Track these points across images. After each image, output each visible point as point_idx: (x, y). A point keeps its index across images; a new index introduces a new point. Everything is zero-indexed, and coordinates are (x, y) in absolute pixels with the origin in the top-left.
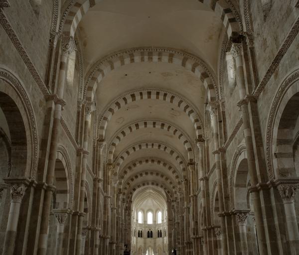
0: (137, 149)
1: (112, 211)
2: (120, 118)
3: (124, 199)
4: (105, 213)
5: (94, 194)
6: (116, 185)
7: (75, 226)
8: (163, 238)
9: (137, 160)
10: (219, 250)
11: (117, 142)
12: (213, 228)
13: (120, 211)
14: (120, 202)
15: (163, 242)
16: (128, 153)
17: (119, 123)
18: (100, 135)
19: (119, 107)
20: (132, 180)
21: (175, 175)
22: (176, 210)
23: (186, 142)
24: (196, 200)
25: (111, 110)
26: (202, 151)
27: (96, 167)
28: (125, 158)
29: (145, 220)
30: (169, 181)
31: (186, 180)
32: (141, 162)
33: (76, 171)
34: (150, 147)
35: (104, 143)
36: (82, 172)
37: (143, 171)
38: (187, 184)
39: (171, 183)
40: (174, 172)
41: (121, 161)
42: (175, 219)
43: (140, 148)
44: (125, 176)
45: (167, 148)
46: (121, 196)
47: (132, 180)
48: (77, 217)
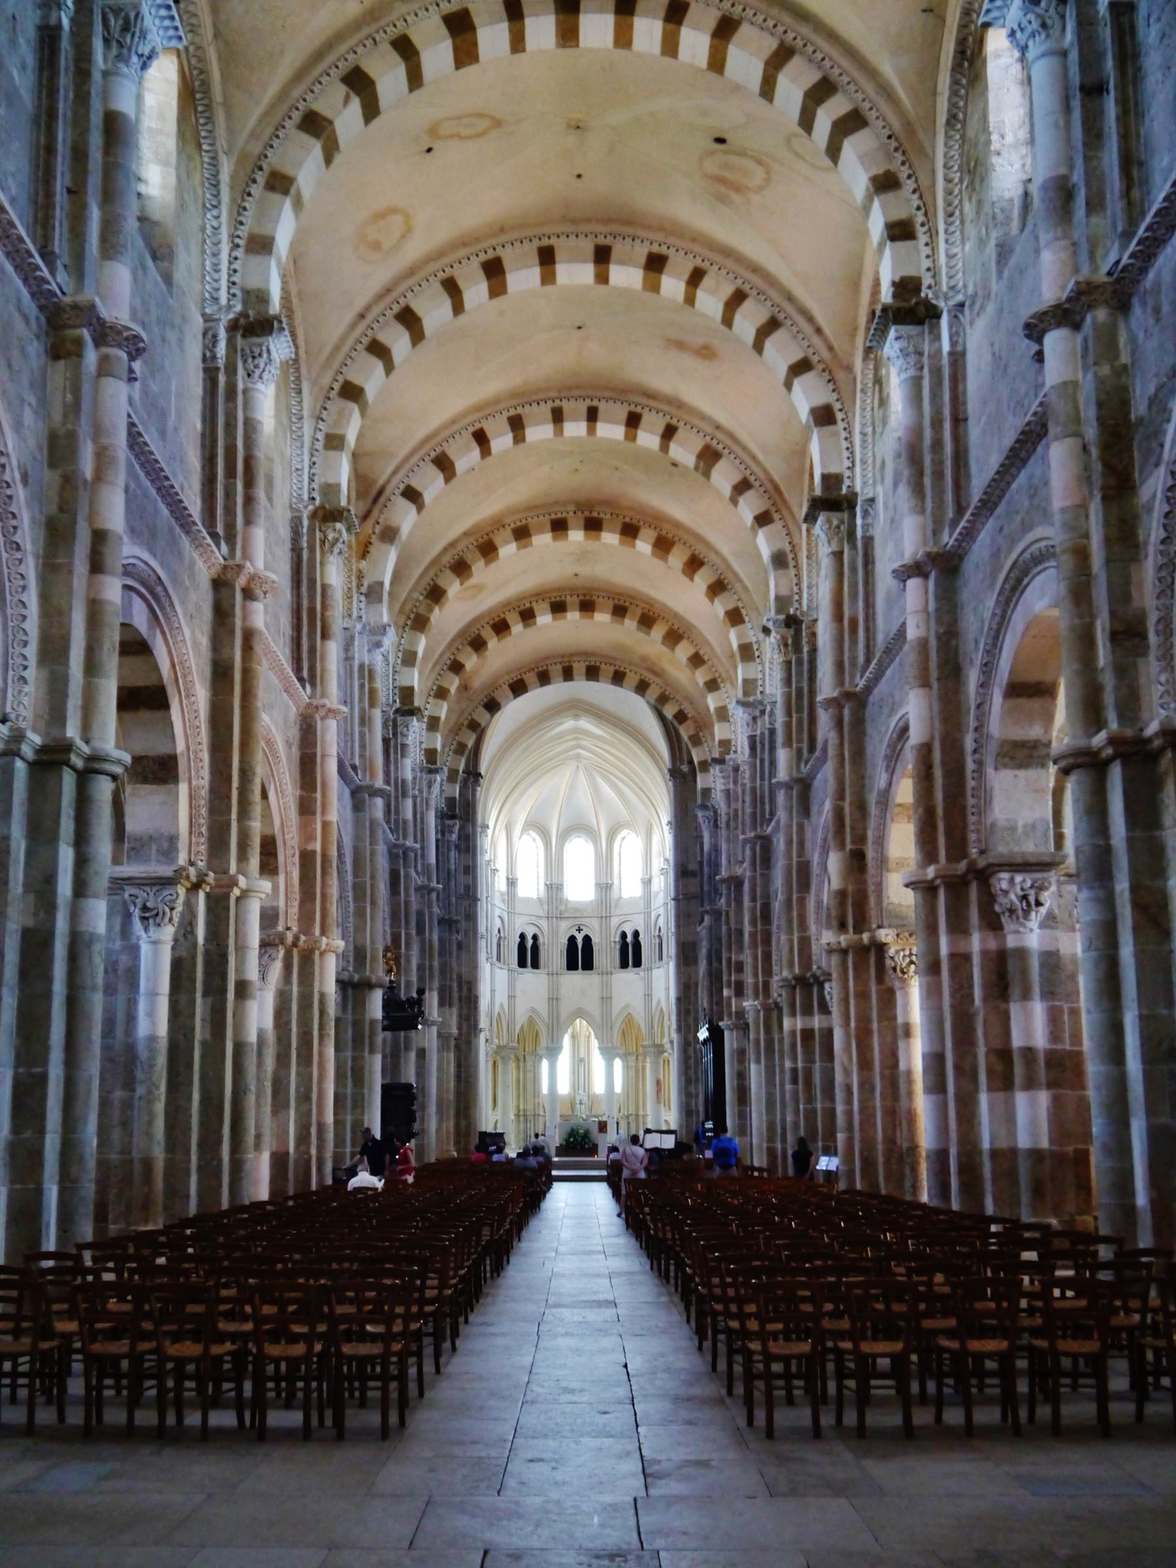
0: (501, 442)
1: (358, 806)
2: (380, 216)
3: (431, 755)
4: (306, 808)
5: (220, 674)
6: (378, 659)
7: (54, 839)
8: (650, 969)
9: (498, 523)
10: (1015, 1009)
11: (372, 378)
12: (984, 875)
13: (409, 815)
14: (409, 767)
15: (648, 996)
16: (444, 464)
17: (376, 246)
18: (247, 292)
19: (371, 111)
20: (478, 645)
21: (720, 608)
22: (723, 808)
23: (801, 367)
24: (859, 723)
25: (314, 124)
26: (915, 384)
27: (229, 494)
28: (428, 497)
29: (554, 888)
30: (683, 651)
31: (792, 622)
32: (522, 534)
33: (52, 464)
34: (575, 429)
35: (279, 347)
36: (99, 477)
37: (539, 595)
38: (798, 649)
39: (696, 660)
40: (717, 588)
41: (405, 518)
42: (715, 866)
43: (519, 438)
44: (436, 615)
45: (681, 434)
46: (415, 732)
47: (478, 645)
48: (68, 780)
